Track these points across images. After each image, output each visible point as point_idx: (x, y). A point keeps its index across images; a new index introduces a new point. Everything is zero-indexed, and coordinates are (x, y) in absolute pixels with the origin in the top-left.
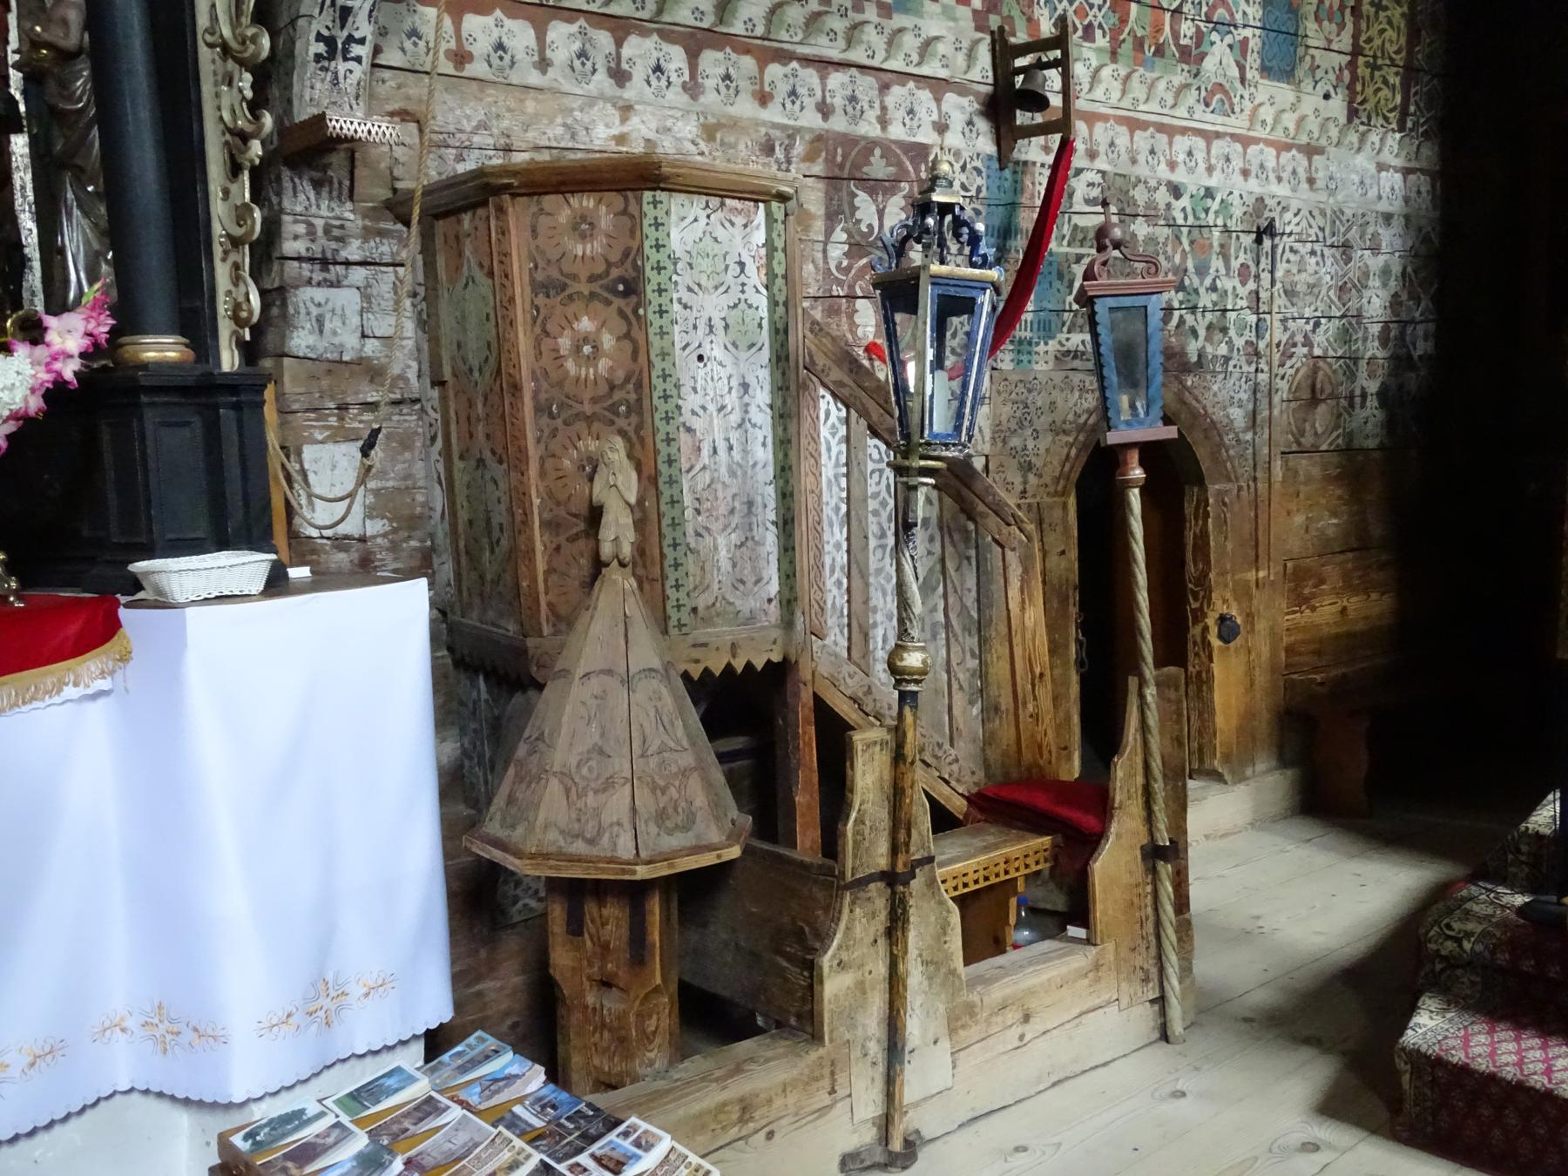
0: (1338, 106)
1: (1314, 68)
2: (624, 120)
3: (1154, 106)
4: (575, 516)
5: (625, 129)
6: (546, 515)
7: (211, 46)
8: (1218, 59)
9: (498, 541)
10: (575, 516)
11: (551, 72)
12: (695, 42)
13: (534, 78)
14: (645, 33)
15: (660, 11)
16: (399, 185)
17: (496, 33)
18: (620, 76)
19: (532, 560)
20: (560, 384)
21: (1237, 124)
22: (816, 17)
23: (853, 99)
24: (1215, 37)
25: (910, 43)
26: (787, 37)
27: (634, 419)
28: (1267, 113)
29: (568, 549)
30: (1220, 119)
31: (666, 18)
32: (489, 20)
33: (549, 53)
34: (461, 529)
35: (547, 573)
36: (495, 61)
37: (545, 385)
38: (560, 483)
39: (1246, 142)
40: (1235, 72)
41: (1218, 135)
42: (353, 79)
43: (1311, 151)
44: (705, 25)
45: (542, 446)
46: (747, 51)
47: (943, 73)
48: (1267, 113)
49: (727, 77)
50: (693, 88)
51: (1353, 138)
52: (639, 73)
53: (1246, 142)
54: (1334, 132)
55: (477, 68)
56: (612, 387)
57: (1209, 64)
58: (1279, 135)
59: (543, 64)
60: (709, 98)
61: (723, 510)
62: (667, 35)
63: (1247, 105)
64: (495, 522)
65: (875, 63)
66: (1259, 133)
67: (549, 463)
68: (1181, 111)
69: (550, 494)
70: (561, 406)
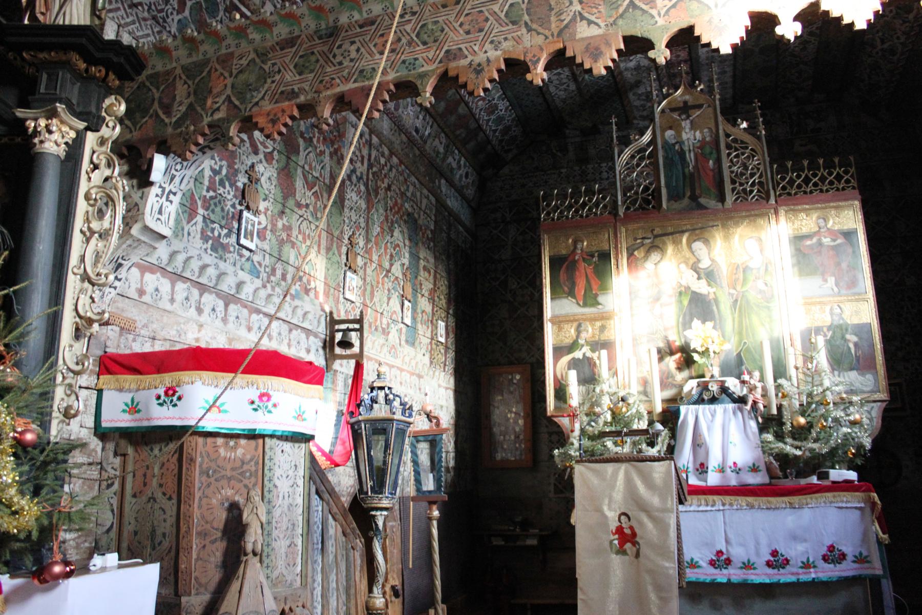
0: (426, 359)
1: (420, 343)
2: (199, 331)
3: (373, 352)
4: (216, 529)
5: (199, 335)
6: (199, 529)
7: (75, 274)
8: (393, 335)
9: (160, 544)
10: (216, 529)
11: (175, 305)
12: (229, 299)
13: (168, 307)
14: (211, 293)
15: (216, 284)
16: (108, 350)
17: (156, 283)
18: (200, 310)
19: (190, 553)
20: (216, 460)
21: (398, 362)
22: (270, 296)
23: (280, 334)
24: (392, 326)
25: (300, 312)
26: (260, 303)
27: (253, 480)
28: (407, 359)
29: (209, 547)
30: (393, 359)
31: (219, 287)
32: (154, 277)
33: (175, 296)
34: (125, 534)
35: (197, 560)
36: (154, 296)
37: (206, 460)
38: (210, 511)
39: (402, 370)
40: (398, 341)
41: (393, 366)
42: (110, 296)
43: (420, 377)
44: (232, 293)
45: (201, 491)
46: (246, 307)
47: (310, 327)
48: (407, 359)
49: (237, 317)
50: (225, 320)
51: (431, 373)
52: (207, 310)
53: (402, 370)
54: (426, 370)
55: (146, 298)
56: (243, 463)
57: (391, 336)
58: (410, 369)
59: (172, 300)
60: (231, 326)
61: (285, 528)
62: (218, 295)
63: (402, 356)
64: (159, 532)
65: (288, 319)
66: (405, 367)
67: (204, 501)
68: (382, 355)
69: (203, 517)
70: (214, 472)
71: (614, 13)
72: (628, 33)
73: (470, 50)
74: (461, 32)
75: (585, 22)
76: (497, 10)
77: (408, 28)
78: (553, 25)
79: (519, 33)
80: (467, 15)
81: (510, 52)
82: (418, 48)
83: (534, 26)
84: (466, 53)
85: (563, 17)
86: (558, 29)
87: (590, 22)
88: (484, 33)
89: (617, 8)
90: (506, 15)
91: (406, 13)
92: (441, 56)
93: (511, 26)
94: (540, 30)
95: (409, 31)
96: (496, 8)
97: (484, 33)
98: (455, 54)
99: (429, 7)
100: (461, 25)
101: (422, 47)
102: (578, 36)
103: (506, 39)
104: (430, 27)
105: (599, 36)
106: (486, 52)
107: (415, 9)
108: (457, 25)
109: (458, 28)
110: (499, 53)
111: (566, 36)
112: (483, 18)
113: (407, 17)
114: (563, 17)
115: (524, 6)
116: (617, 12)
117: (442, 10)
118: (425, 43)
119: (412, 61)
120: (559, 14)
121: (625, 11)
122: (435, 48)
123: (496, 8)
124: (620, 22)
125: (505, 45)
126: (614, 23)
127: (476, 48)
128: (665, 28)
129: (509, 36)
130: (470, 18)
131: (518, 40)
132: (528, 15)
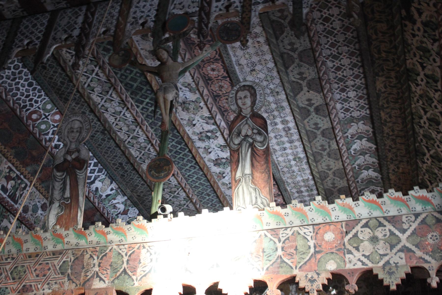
71: (114, 275)
72: (119, 289)
73: (36, 287)
74: (34, 275)
75: (98, 278)
76: (56, 264)
77: (8, 267)
78: (82, 278)
79: (63, 280)
80: (40, 264)
81: (56, 291)
82: (9, 281)
83: (72, 277)
84: (34, 288)
85: (88, 274)
86: (84, 281)
87: (101, 279)
88: (45, 277)
89: (116, 272)
90: (60, 269)
91: (9, 258)
92: (20, 288)
93: (60, 276)
94: (75, 280)
95: (7, 269)
96: (56, 262)
97: (45, 277)
98: (28, 289)
99: (22, 256)
100: (35, 270)
101: (12, 281)
102: (93, 287)
103: (56, 283)
104: (19, 268)
105: (103, 288)
106: (44, 290)
107: (15, 256)
108: (33, 270)
109: (33, 272)
110: (50, 291)
111: (87, 285)
112: (48, 268)
113: (9, 260)
114: (88, 274)
115: (70, 264)
116: (116, 275)
117: (28, 259)
118: (14, 279)
119: (4, 289)
120: (87, 272)
121: (120, 275)
122: (18, 283)
123: (56, 262)
124: (116, 281)
125: (55, 287)
126: (113, 282)
127: (39, 286)
128: (138, 289)
129: (58, 281)
130: (41, 266)
131: (62, 285)
132: (71, 270)
